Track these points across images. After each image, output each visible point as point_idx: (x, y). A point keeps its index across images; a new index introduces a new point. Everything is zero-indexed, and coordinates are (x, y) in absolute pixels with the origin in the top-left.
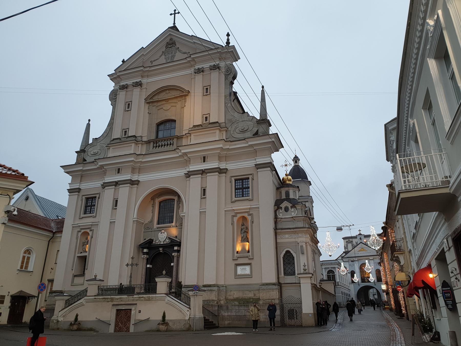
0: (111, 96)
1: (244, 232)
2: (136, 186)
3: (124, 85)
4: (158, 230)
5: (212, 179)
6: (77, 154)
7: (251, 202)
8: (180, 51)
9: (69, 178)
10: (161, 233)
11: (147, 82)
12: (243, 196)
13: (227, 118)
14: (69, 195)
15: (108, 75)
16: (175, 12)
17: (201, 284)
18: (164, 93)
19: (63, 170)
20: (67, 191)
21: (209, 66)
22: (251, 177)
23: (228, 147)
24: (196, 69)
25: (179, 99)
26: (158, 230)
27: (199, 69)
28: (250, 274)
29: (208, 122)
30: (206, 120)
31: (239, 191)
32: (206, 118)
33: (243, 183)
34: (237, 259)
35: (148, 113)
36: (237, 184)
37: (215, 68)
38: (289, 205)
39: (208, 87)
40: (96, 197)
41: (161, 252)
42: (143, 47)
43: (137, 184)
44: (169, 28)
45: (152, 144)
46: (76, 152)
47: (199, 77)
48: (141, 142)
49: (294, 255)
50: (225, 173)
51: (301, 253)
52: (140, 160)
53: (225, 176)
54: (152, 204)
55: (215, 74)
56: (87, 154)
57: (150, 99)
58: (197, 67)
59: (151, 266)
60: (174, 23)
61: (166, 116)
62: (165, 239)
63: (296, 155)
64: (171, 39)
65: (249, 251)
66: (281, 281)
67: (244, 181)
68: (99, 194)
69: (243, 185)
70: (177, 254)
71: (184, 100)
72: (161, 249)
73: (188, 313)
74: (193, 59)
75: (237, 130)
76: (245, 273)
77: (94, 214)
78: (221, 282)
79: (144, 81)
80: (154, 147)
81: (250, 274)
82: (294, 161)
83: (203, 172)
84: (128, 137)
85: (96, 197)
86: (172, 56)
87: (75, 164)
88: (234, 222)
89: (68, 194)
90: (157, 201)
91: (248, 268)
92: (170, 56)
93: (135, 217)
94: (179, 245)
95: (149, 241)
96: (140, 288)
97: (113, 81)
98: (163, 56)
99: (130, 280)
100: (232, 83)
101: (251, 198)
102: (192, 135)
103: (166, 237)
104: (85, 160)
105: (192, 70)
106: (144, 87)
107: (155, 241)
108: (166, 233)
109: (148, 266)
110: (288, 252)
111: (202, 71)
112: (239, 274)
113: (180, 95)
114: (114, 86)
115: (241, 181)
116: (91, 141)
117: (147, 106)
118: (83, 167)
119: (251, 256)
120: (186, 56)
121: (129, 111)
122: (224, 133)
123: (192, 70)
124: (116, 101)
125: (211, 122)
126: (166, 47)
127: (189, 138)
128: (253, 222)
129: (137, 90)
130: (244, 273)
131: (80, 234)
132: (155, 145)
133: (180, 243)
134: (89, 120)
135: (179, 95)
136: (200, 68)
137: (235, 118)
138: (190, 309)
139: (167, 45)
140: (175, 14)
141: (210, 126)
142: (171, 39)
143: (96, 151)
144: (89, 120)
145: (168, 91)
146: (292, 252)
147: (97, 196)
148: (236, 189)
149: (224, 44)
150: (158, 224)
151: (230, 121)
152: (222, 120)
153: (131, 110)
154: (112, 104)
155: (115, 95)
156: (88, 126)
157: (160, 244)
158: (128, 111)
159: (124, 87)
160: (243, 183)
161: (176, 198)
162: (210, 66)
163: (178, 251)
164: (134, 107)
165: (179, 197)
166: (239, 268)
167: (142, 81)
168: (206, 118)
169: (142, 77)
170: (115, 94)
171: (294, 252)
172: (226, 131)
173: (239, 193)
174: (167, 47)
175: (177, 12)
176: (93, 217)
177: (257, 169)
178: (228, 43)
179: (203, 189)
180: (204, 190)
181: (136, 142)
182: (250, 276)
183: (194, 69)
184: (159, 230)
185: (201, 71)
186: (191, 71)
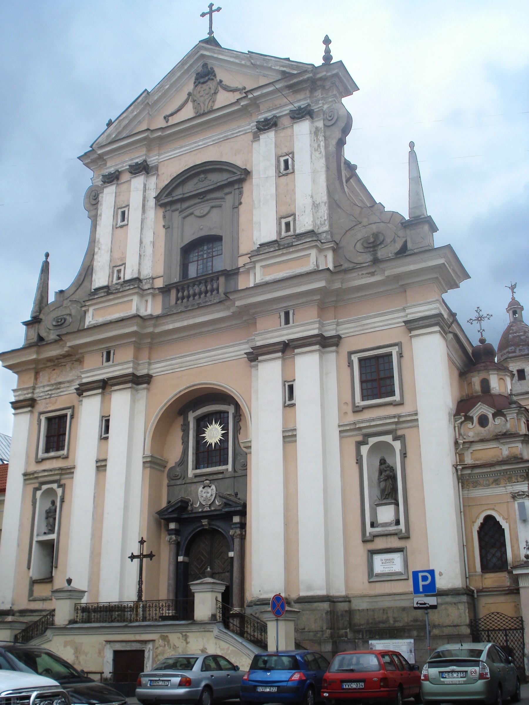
2: (145, 386)
3: (112, 174)
4: (196, 480)
9: (13, 378)
10: (203, 486)
11: (159, 161)
14: (14, 414)
18: (195, 180)
20: (10, 405)
22: (397, 349)
23: (337, 285)
25: (227, 190)
26: (196, 480)
27: (266, 120)
28: (403, 572)
29: (291, 233)
30: (288, 229)
31: (369, 385)
32: (288, 225)
34: (372, 540)
35: (164, 226)
38: (489, 412)
40: (65, 416)
41: (205, 528)
42: (146, 90)
43: (148, 383)
44: (200, 42)
45: (173, 292)
48: (151, 291)
49: (504, 525)
50: (337, 345)
51: (520, 519)
52: (150, 330)
53: (337, 352)
57: (166, 196)
58: (261, 117)
59: (187, 559)
60: (211, 32)
61: (201, 229)
62: (213, 499)
63: (513, 299)
64: (205, 65)
65: (399, 522)
68: (72, 408)
70: (239, 532)
71: (237, 192)
75: (359, 247)
76: (392, 569)
77: (65, 452)
79: (152, 160)
80: (177, 299)
81: (403, 572)
82: (511, 312)
84: (123, 282)
85: (65, 416)
87: (21, 346)
88: (362, 456)
89: (13, 411)
90: (192, 417)
91: (397, 557)
95: (179, 504)
96: (160, 608)
97: (90, 168)
99: (139, 589)
100: (341, 143)
102: (258, 266)
103: (214, 497)
104: (41, 339)
108: (213, 487)
109: (181, 559)
110: (489, 519)
111: (273, 125)
112: (379, 572)
113: (229, 180)
116: (51, 298)
117: (161, 212)
118: (38, 353)
119: (404, 531)
120: (237, 95)
121: (125, 228)
122: (330, 255)
123: (252, 125)
125: (298, 231)
126: (195, 83)
128: (404, 454)
129: (138, 182)
130: (389, 569)
131: (39, 493)
132: (180, 294)
134: (47, 255)
139: (196, 79)
140: (211, 12)
142: (205, 65)
144: (47, 255)
145: (202, 176)
146: (499, 518)
147: (69, 412)
149: (319, 62)
153: (128, 225)
157: (202, 512)
158: (122, 227)
161: (231, 410)
162: (291, 111)
163: (243, 526)
166: (378, 559)
167: (148, 160)
168: (288, 225)
169: (149, 150)
170: (94, 194)
171: (504, 518)
172: (334, 250)
174: (197, 83)
176: (63, 458)
177: (410, 330)
178: (328, 57)
179: (287, 384)
180: (291, 388)
181: (141, 292)
183: (257, 122)
185: (271, 125)
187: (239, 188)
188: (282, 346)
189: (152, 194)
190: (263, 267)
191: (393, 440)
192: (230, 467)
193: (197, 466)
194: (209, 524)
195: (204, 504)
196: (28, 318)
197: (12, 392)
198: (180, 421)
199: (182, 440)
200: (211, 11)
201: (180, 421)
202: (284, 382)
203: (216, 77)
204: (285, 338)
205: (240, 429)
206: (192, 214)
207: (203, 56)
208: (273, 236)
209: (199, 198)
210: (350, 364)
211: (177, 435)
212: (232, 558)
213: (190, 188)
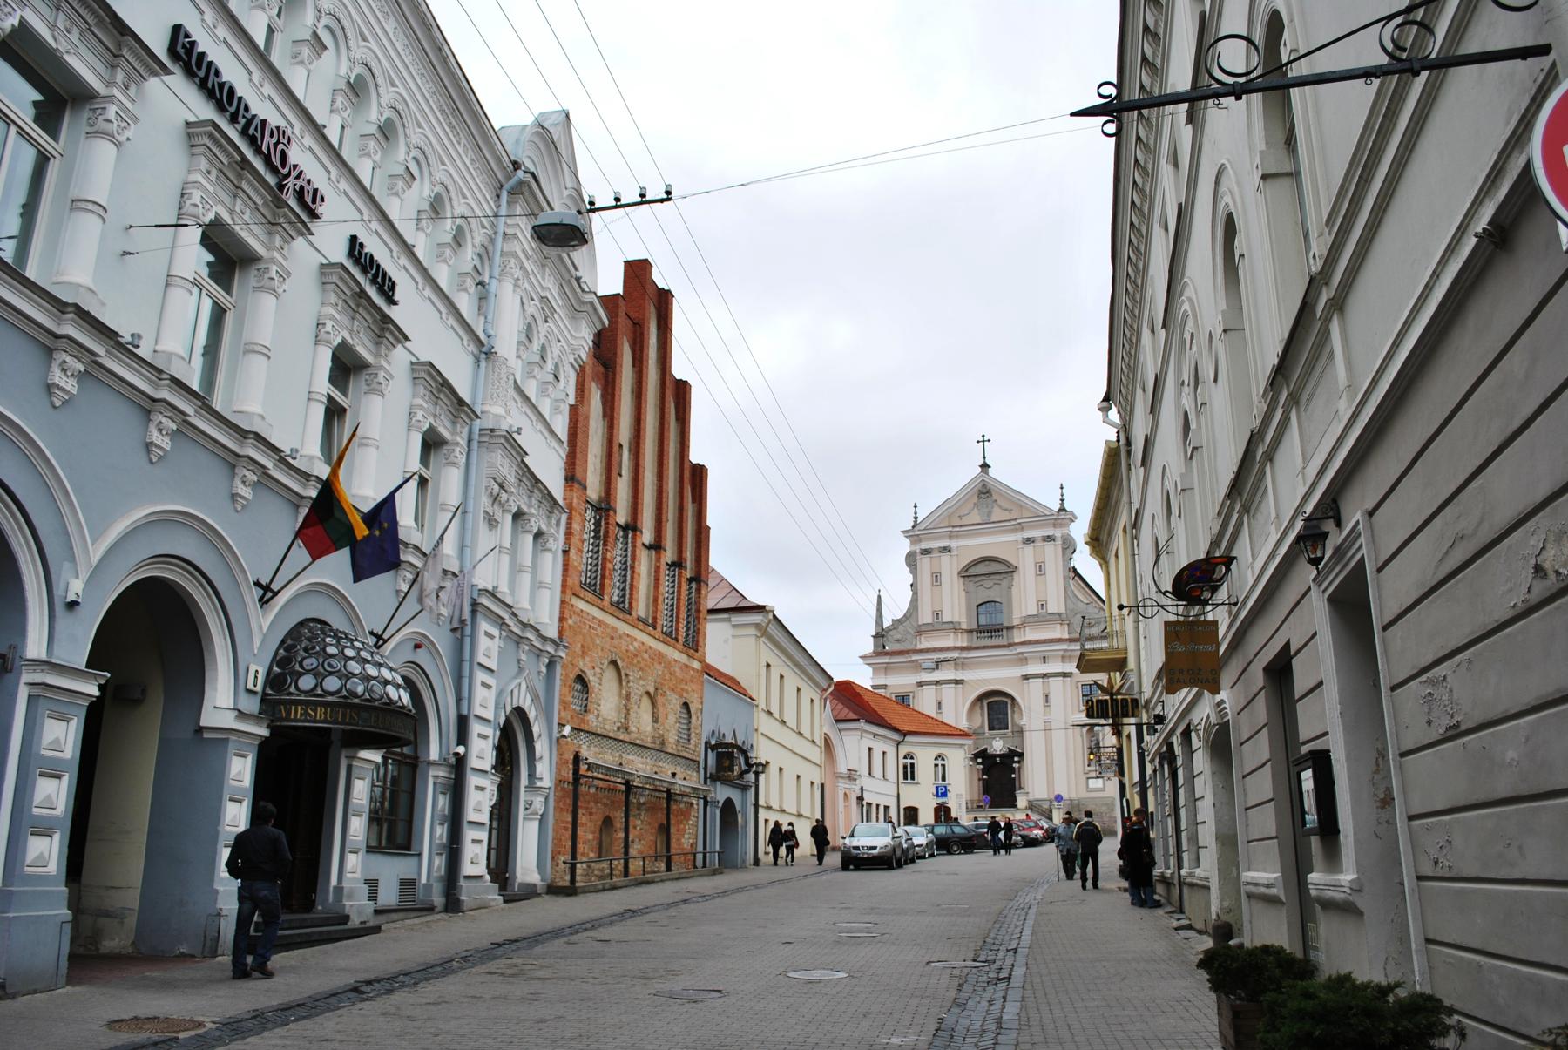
5: (1056, 685)
8: (1000, 507)
18: (983, 564)
37: (1049, 538)
47: (1029, 548)
55: (1049, 546)
64: (984, 485)
74: (1019, 524)
78: (1073, 796)
79: (954, 544)
94: (1021, 755)
106: (954, 553)
117: (962, 580)
124: (916, 569)
125: (1049, 611)
129: (945, 558)
141: (1049, 617)
143: (899, 637)
147: (911, 695)
151: (1072, 610)
152: (1063, 610)
156: (879, 597)
159: (926, 552)
161: (1009, 701)
164: (945, 579)
165: (1013, 699)
182: (1103, 790)
193: (990, 729)
196: (874, 634)
198: (979, 704)
208: (1035, 613)
211: (978, 710)
213: (980, 569)
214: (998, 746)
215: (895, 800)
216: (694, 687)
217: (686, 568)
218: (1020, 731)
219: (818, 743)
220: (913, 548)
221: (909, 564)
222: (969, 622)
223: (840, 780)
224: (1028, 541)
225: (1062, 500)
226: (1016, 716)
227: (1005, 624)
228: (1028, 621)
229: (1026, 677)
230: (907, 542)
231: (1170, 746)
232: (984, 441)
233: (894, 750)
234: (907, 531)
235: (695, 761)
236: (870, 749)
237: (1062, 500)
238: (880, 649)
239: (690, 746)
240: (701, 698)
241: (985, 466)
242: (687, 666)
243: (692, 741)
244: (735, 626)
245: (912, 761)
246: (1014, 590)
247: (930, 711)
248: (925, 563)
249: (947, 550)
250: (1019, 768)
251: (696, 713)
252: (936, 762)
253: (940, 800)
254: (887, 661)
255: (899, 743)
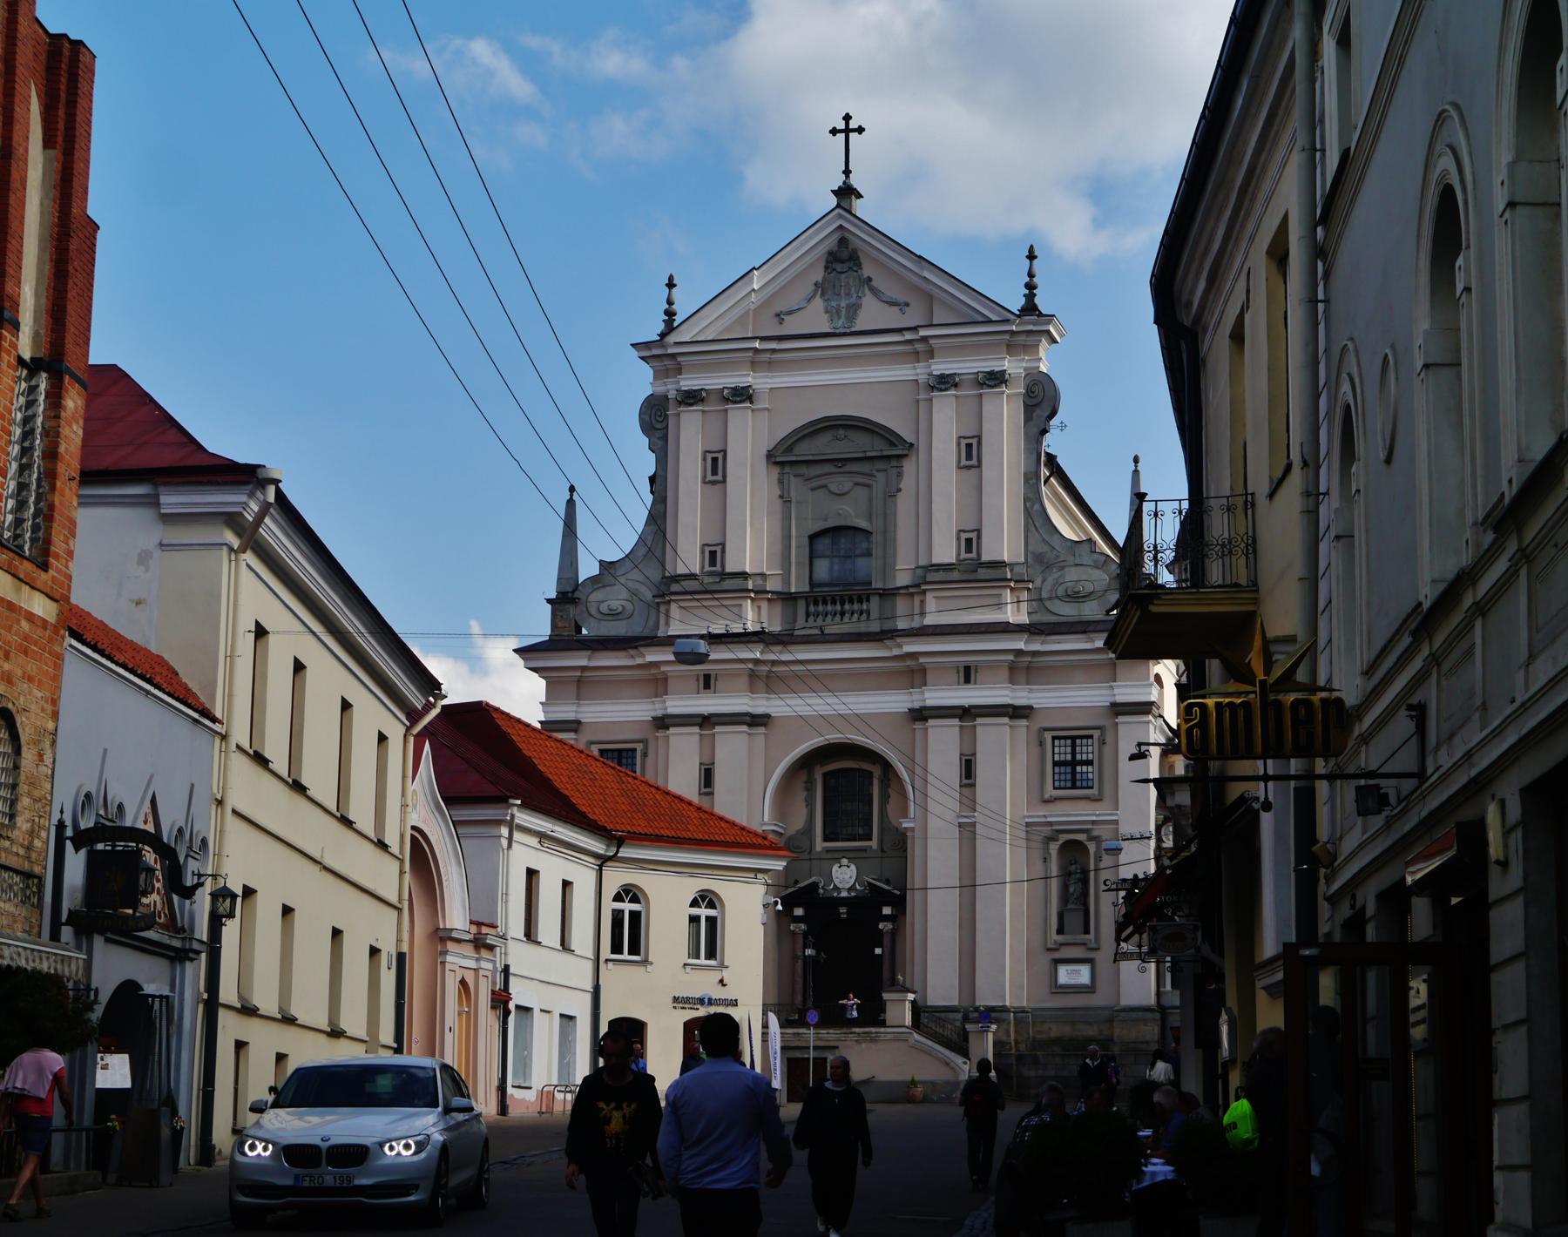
0: (647, 418)
1: (1075, 883)
4: (829, 856)
6: (550, 606)
7: (1097, 805)
8: (875, 292)
12: (1074, 787)
13: (1030, 548)
15: (632, 345)
16: (847, 124)
17: (965, 1004)
18: (828, 436)
19: (522, 662)
21: (976, 371)
24: (934, 373)
25: (880, 465)
29: (974, 555)
30: (969, 550)
32: (969, 541)
33: (1074, 746)
36: (1057, 750)
39: (974, 442)
46: (549, 601)
50: (1026, 717)
54: (806, 782)
56: (585, 609)
57: (784, 452)
60: (847, 172)
61: (839, 515)
64: (843, 242)
66: (1166, 1002)
67: (1078, 741)
69: (1074, 753)
71: (895, 471)
72: (843, 910)
73: (966, 1068)
74: (925, 339)
80: (808, 615)
83: (966, 713)
86: (849, 307)
88: (1050, 854)
92: (843, 304)
93: (766, 819)
94: (900, 903)
98: (818, 302)
100: (1044, 431)
101: (1097, 793)
102: (929, 596)
105: (918, 371)
107: (823, 888)
109: (809, 952)
113: (885, 453)
114: (651, 380)
115: (1069, 742)
117: (776, 471)
118: (590, 659)
123: (918, 371)
124: (665, 438)
125: (985, 558)
126: (826, 268)
127: (917, 599)
129: (740, 418)
132: (812, 609)
133: (902, 899)
135: (879, 454)
136: (947, 372)
137: (1055, 553)
138: (970, 1060)
143: (616, 604)
145: (841, 432)
147: (639, 747)
148: (1055, 764)
150: (826, 839)
153: (724, 481)
154: (653, 447)
155: (660, 416)
156: (571, 504)
157: (837, 898)
159: (692, 398)
160: (1074, 746)
161: (877, 771)
165: (886, 766)
170: (659, 413)
173: (1063, 777)
175: (853, 125)
177: (1117, 714)
179: (964, 758)
182: (1090, 989)
184: (835, 856)
186: (913, 372)
187: (897, 467)
188: (961, 711)
189: (766, 444)
190: (934, 597)
191: (1088, 841)
192: (874, 844)
193: (826, 839)
194: (848, 913)
195: (840, 886)
196: (553, 595)
197: (540, 706)
198: (803, 776)
199: (806, 801)
200: (847, 129)
201: (803, 776)
202: (961, 755)
203: (861, 269)
204: (966, 702)
205: (889, 797)
206: (825, 486)
207: (841, 226)
209: (836, 466)
210: (1041, 744)
211: (802, 795)
212: (880, 956)
214: (844, 876)
215: (588, 998)
216: (32, 667)
217: (16, 326)
218: (898, 845)
219: (395, 849)
220: (660, 389)
221: (647, 428)
222: (786, 578)
223: (450, 946)
224: (945, 382)
225: (1031, 287)
226: (890, 807)
227: (877, 584)
228: (930, 576)
229: (920, 715)
230: (646, 372)
231: (1473, 835)
232: (847, 131)
233: (591, 876)
234: (647, 345)
235: (27, 876)
236: (532, 874)
237: (1031, 287)
238: (569, 632)
239: (16, 834)
240: (54, 702)
241: (846, 193)
242: (11, 606)
243: (19, 820)
244: (169, 519)
245: (635, 907)
246: (903, 504)
247: (682, 780)
248: (691, 431)
249: (742, 395)
250: (894, 933)
251: (37, 742)
252: (695, 911)
253: (706, 1000)
254: (584, 662)
255: (603, 861)
